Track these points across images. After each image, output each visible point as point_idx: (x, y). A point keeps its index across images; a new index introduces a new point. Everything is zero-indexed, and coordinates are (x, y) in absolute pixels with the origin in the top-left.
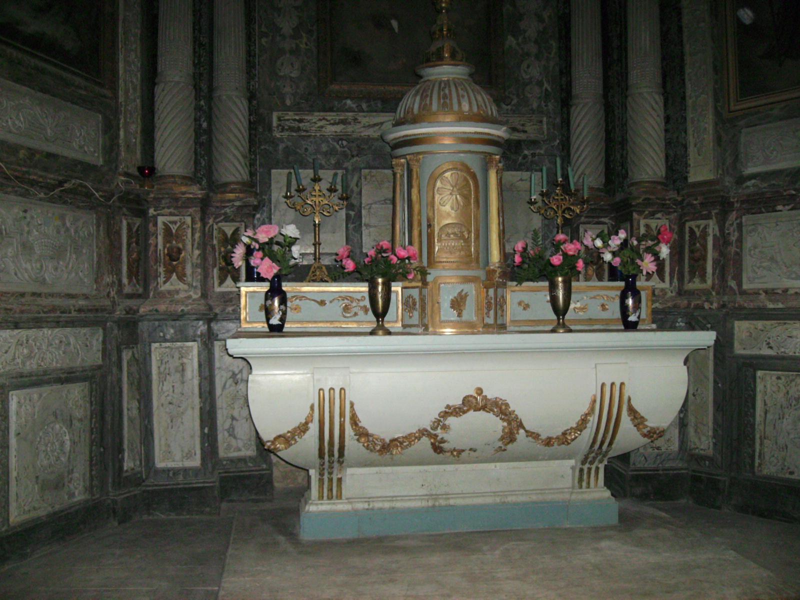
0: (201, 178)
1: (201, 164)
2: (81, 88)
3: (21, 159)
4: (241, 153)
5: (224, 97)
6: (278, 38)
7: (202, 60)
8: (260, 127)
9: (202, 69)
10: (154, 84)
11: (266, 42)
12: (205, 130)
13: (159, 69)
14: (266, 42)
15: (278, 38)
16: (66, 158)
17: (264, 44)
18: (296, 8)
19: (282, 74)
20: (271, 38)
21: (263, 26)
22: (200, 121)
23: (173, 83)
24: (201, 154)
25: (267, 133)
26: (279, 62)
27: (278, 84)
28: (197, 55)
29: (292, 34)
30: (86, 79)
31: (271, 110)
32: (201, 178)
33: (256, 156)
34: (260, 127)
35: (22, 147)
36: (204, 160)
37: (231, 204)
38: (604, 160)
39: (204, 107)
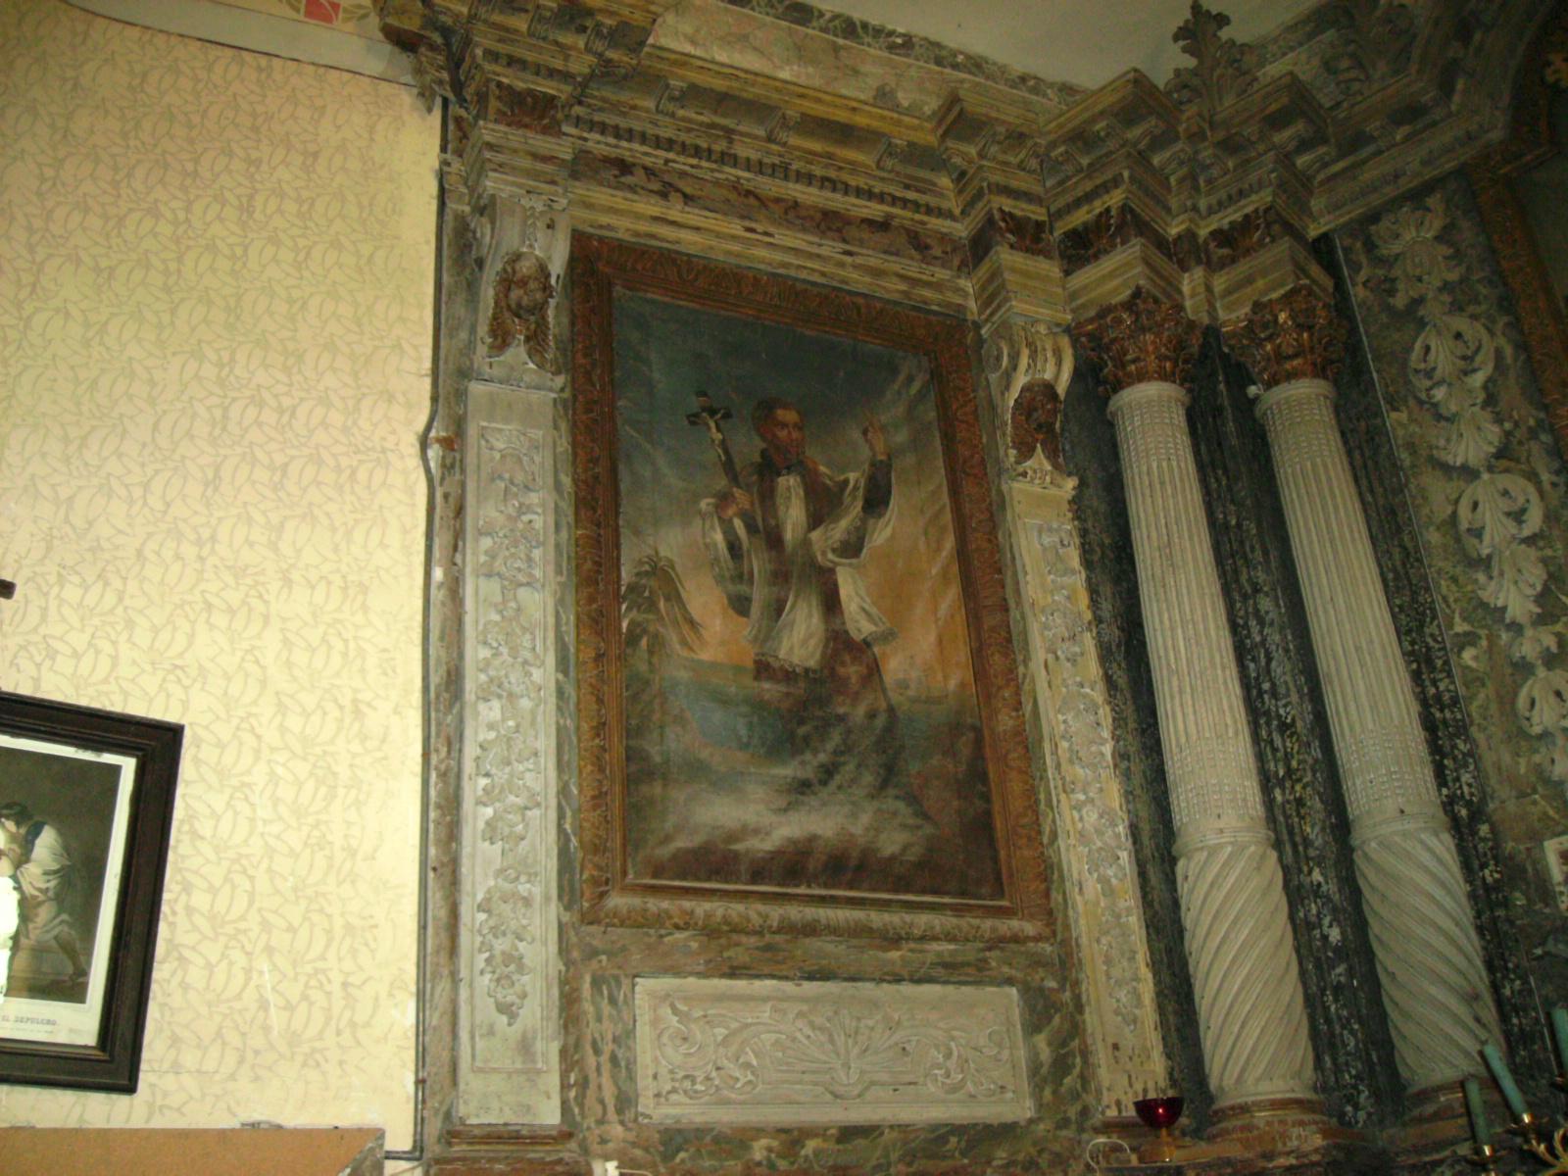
0: (1355, 1087)
1: (1345, 1045)
2: (935, 938)
3: (759, 1164)
4: (1451, 988)
5: (1373, 844)
6: (1505, 636)
7: (1294, 764)
8: (1517, 894)
9: (1298, 787)
10: (1173, 861)
11: (1476, 658)
12: (1336, 950)
13: (1176, 823)
14: (1476, 658)
15: (1505, 636)
16: (903, 1128)
17: (1473, 664)
18: (1530, 541)
19: (1537, 730)
20: (1484, 643)
21: (1457, 619)
22: (1320, 926)
23: (1205, 854)
24: (1340, 1018)
25: (1539, 906)
26: (1522, 702)
27: (1537, 758)
28: (1280, 755)
29: (1538, 610)
30: (958, 910)
31: (1536, 838)
32: (1355, 1087)
33: (1526, 982)
34: (1517, 894)
35: (759, 1131)
36: (1353, 1032)
37: (1446, 1153)
38: (1202, 1028)
39: (1324, 888)
